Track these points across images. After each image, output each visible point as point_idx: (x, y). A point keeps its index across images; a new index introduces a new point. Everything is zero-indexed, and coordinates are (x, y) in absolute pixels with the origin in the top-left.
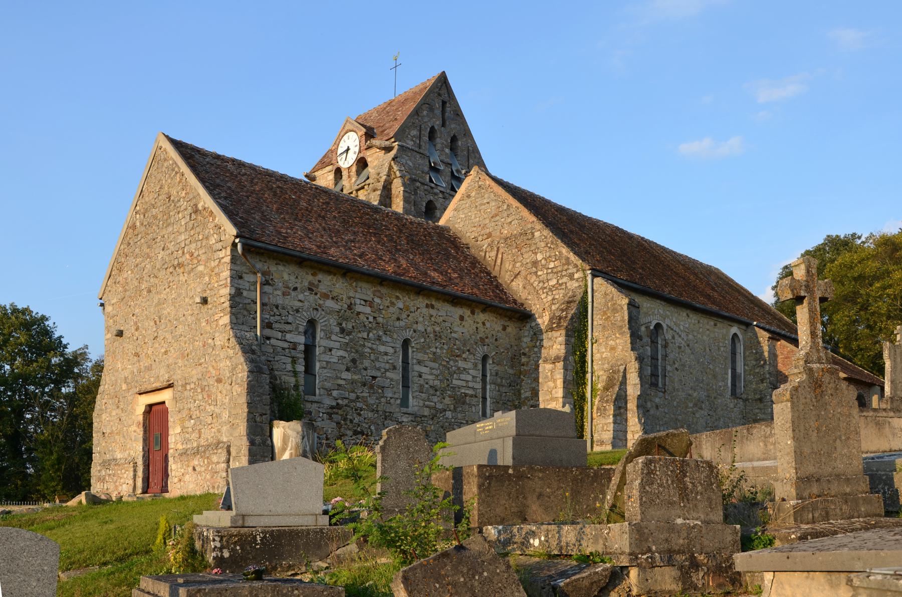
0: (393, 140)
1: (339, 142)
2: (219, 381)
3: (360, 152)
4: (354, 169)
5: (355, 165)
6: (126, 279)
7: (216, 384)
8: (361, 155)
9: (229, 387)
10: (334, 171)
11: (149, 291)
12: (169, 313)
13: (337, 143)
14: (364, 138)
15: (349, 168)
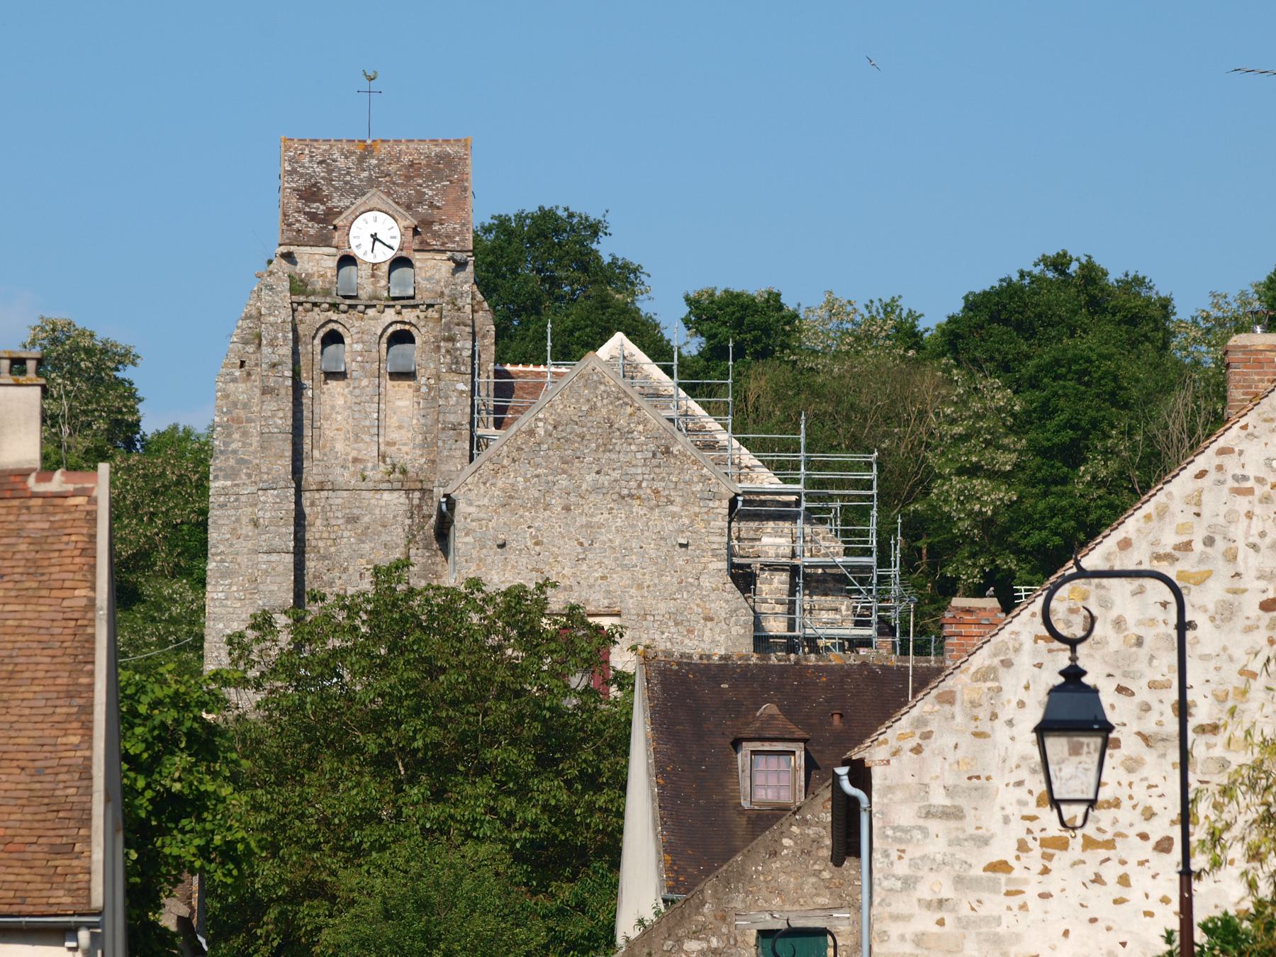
0: (470, 254)
1: (354, 219)
2: (708, 619)
3: (401, 249)
4: (385, 268)
5: (388, 263)
6: (513, 485)
7: (702, 621)
8: (404, 254)
9: (725, 627)
10: (337, 258)
11: (567, 509)
12: (610, 540)
13: (351, 219)
14: (410, 233)
15: (374, 264)
